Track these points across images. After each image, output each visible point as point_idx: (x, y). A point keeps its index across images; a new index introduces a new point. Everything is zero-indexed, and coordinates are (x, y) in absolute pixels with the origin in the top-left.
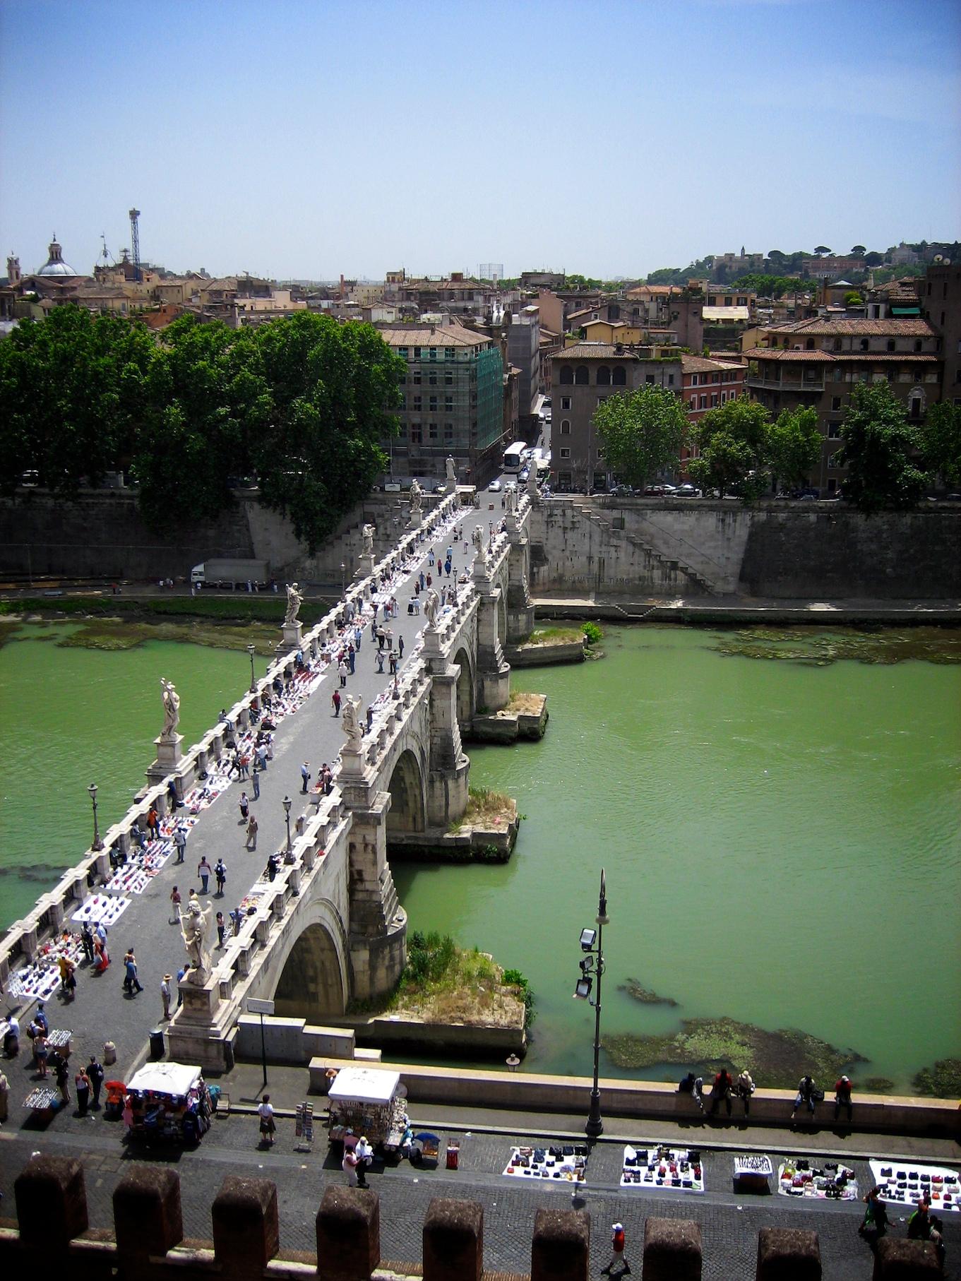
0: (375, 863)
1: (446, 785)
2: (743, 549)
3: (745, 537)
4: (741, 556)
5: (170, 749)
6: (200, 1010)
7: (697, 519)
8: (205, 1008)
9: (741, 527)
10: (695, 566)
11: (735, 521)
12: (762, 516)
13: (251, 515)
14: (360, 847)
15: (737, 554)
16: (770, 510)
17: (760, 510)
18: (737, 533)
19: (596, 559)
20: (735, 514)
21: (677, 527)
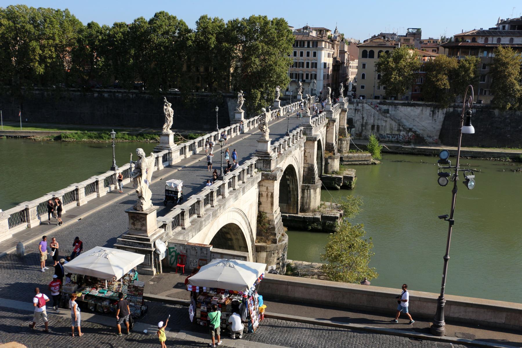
0: (272, 204)
1: (310, 191)
2: (441, 124)
3: (442, 119)
4: (440, 127)
5: (167, 137)
6: (140, 230)
7: (422, 110)
8: (144, 228)
9: (440, 115)
10: (419, 132)
11: (438, 112)
12: (451, 110)
13: (229, 104)
14: (264, 194)
15: (438, 126)
16: (454, 107)
17: (450, 107)
18: (439, 117)
19: (376, 126)
20: (438, 109)
21: (412, 113)
